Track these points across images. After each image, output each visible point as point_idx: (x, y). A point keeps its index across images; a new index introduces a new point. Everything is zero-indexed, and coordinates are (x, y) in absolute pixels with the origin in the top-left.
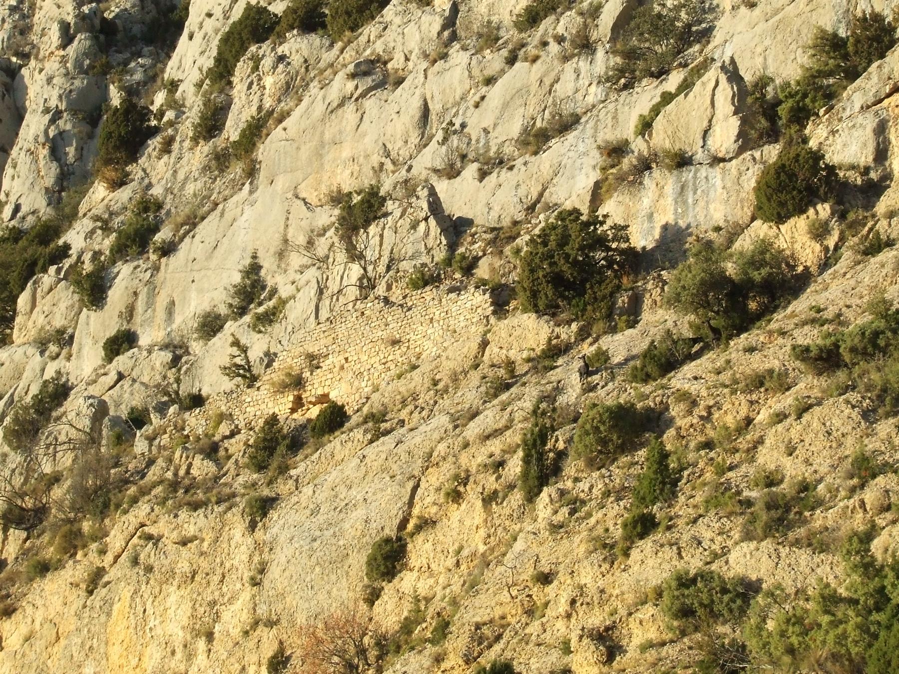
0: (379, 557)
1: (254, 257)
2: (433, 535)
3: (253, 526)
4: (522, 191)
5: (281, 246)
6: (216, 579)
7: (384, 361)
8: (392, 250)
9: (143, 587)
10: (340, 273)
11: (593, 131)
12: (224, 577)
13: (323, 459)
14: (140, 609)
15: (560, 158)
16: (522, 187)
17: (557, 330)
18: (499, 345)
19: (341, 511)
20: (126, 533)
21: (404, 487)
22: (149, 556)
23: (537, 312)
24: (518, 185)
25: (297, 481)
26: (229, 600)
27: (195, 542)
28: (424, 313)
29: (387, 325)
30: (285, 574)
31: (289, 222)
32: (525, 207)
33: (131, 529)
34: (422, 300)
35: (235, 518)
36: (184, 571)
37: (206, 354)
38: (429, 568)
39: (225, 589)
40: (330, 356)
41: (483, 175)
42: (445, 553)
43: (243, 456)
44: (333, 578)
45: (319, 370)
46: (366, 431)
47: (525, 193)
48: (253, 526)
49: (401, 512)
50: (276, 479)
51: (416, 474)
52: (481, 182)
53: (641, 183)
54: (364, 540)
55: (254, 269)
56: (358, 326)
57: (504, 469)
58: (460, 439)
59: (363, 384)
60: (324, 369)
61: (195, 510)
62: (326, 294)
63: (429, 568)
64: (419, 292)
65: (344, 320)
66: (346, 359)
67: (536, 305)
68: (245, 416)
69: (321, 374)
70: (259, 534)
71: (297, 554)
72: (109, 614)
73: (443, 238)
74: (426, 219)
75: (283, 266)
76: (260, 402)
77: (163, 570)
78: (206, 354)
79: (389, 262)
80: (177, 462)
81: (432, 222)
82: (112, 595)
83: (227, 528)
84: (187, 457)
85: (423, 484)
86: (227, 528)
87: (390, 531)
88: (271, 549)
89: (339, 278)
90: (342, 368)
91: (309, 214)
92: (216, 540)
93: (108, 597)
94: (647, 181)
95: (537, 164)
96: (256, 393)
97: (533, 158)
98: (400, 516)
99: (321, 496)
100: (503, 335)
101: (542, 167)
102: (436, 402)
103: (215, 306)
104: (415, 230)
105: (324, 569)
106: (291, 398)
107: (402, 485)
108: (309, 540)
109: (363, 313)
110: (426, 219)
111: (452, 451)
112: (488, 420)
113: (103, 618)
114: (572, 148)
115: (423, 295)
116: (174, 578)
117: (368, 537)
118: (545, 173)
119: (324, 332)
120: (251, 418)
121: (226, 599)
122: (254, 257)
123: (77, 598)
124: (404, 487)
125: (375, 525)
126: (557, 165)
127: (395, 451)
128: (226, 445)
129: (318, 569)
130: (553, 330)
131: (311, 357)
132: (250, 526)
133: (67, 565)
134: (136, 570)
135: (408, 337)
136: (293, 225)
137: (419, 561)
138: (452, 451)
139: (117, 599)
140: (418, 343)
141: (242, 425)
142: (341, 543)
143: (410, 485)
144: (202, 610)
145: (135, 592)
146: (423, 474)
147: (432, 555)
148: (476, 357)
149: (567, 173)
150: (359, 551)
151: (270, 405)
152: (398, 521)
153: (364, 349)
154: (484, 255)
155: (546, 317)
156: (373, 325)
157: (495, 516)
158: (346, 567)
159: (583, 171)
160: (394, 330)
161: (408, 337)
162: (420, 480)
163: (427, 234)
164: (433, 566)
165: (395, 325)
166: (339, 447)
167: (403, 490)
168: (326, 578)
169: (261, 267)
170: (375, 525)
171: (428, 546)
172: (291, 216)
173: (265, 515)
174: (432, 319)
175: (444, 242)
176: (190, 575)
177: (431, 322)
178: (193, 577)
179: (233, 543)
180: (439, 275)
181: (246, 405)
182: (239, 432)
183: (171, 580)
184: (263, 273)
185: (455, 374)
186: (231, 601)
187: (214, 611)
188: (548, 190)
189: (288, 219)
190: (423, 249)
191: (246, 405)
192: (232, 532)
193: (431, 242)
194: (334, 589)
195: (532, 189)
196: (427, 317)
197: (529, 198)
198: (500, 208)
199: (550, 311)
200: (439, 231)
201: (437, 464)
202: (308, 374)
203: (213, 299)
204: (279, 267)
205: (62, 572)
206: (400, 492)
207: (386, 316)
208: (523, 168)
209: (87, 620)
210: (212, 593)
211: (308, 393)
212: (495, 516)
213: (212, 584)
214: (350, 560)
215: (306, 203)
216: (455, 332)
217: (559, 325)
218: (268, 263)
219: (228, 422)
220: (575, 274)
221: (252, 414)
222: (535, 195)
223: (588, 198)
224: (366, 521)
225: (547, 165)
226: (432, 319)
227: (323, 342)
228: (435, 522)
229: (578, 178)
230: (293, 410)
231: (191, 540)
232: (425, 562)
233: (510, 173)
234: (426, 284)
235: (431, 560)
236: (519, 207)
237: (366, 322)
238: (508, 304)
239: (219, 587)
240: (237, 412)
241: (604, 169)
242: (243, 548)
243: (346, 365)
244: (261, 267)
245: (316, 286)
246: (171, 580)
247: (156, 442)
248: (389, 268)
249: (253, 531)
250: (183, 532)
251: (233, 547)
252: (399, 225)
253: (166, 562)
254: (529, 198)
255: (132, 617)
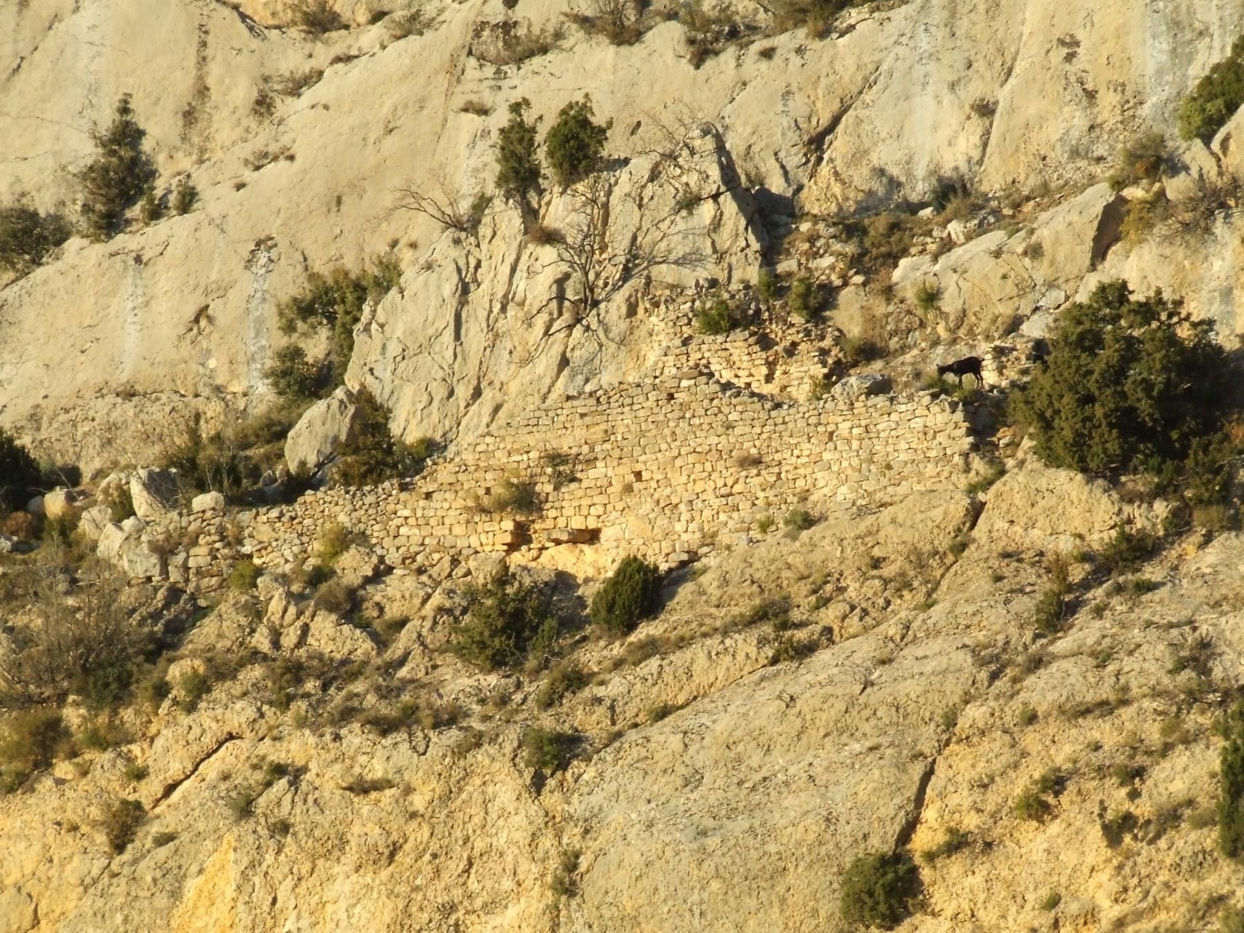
0: (879, 891)
1: (125, 110)
2: (988, 865)
3: (538, 783)
4: (798, 105)
5: (190, 99)
6: (455, 866)
7: (724, 491)
8: (635, 238)
9: (269, 858)
10: (510, 259)
11: (945, 14)
12: (470, 864)
13: (667, 677)
14: (261, 897)
15: (877, 57)
16: (797, 97)
17: (1127, 509)
18: (1009, 517)
19: (753, 789)
20: (195, 748)
21: (905, 771)
22: (279, 804)
23: (1084, 470)
24: (788, 93)
25: (612, 708)
26: (485, 905)
27: (388, 792)
28: (813, 420)
29: (730, 427)
30: (639, 885)
31: (209, 52)
32: (806, 138)
33: (209, 741)
34: (723, 354)
35: (497, 765)
36: (371, 841)
37: (26, 298)
38: (973, 916)
39: (473, 885)
40: (599, 464)
41: (701, 53)
42: (1019, 899)
43: (432, 629)
44: (751, 903)
45: (573, 485)
46: (762, 642)
47: (804, 111)
48: (538, 783)
49: (903, 813)
50: (561, 697)
51: (927, 751)
52: (697, 67)
53: (1207, 230)
54: (823, 850)
55: (127, 134)
56: (661, 418)
57: (1143, 781)
58: (1016, 704)
59: (679, 527)
60: (585, 484)
61: (384, 733)
62: (479, 297)
63: (973, 916)
64: (720, 339)
65: (628, 401)
66: (638, 475)
67: (1082, 459)
68: (398, 542)
69: (580, 493)
70: (551, 799)
71: (669, 853)
72: (176, 895)
73: (751, 238)
74: (715, 197)
75: (196, 140)
76: (433, 522)
77: (317, 833)
78: (26, 298)
79: (628, 261)
80: (276, 619)
81: (729, 205)
82: (182, 861)
83: (477, 781)
84: (300, 613)
85: (941, 771)
86: (477, 781)
87: (881, 842)
88: (587, 831)
89: (506, 269)
90: (628, 489)
91: (255, 43)
92: (448, 796)
93: (171, 863)
94: (1219, 227)
95: (825, 60)
96: (422, 503)
97: (817, 44)
98: (901, 819)
99: (701, 756)
100: (1017, 502)
101: (838, 66)
102: (888, 603)
103: (23, 195)
104: (690, 213)
105: (729, 887)
106: (508, 525)
107: (901, 768)
108: (691, 832)
109: (671, 397)
110: (715, 197)
111: (999, 723)
112: (1072, 680)
113: (162, 901)
114: (904, 40)
115: (727, 345)
116: (342, 850)
117: (830, 846)
118: (847, 79)
119: (582, 415)
120: (414, 549)
121: (478, 903)
122: (125, 110)
123: (86, 857)
124: (905, 771)
125: (848, 828)
126: (871, 67)
127: (862, 699)
128: (377, 598)
129: (715, 885)
130: (1120, 509)
131: (556, 459)
132: (533, 784)
133: (39, 787)
134: (251, 824)
135: (777, 457)
136: (219, 58)
137: (954, 904)
138: (999, 723)
139: (194, 869)
140: (802, 471)
141: (393, 558)
142: (772, 848)
143: (917, 770)
144: (425, 917)
145: (252, 865)
146: (939, 752)
147: (982, 897)
148: (959, 530)
149: (895, 88)
150: (810, 866)
151: (459, 530)
152: (898, 829)
153: (678, 462)
154: (845, 284)
155: (1100, 481)
156: (696, 421)
157: (1139, 860)
158: (781, 889)
159: (929, 89)
160: (747, 440)
161: (777, 457)
162: (934, 761)
163: (717, 224)
164: (981, 914)
165: (748, 429)
166: (701, 661)
167: (905, 778)
168: (732, 902)
169: (141, 133)
170: (848, 828)
171: (977, 880)
172: (210, 39)
173: (563, 766)
174: (832, 433)
175: (756, 245)
176: (387, 852)
177: (831, 439)
178: (392, 855)
179: (494, 809)
180: (758, 312)
181: (397, 521)
182: (390, 570)
183: (336, 853)
184: (146, 145)
185: (919, 555)
186: (490, 907)
187: (451, 921)
188: (851, 112)
189: (204, 44)
190: (709, 250)
191: (397, 521)
192: (490, 789)
193: (724, 238)
194: (751, 923)
195: (819, 105)
196: (821, 429)
197: (814, 122)
198: (749, 130)
199: (1109, 473)
200: (743, 222)
201: (967, 738)
202: (549, 488)
203: (18, 180)
204: (184, 138)
205: (32, 800)
206: (898, 780)
207: (725, 410)
208: (796, 60)
209: (121, 900)
210: (447, 889)
211: (549, 523)
212: (1139, 860)
213: (445, 876)
214: (790, 879)
215: (244, 17)
216: (889, 467)
217: (1131, 501)
218: (158, 128)
219: (362, 549)
220: (1157, 416)
221: (416, 540)
222: (825, 120)
223: (1091, 232)
224: (828, 820)
225: (851, 62)
226: (832, 433)
227: (581, 433)
228: (988, 845)
229: (917, 100)
230: (512, 547)
231: (378, 786)
232: (965, 906)
233: (764, 65)
234: (734, 325)
235: (979, 905)
236: (793, 136)
237: (677, 414)
238: (994, 431)
239: (461, 880)
240: (376, 532)
241: (953, 86)
242: (519, 820)
243: (637, 486)
244: (141, 133)
245: (455, 278)
246: (336, 853)
247: (179, 559)
248: (627, 274)
249: (539, 793)
250: (357, 770)
251: (495, 816)
252: (647, 193)
253: (325, 820)
254: (814, 122)
255: (241, 907)
